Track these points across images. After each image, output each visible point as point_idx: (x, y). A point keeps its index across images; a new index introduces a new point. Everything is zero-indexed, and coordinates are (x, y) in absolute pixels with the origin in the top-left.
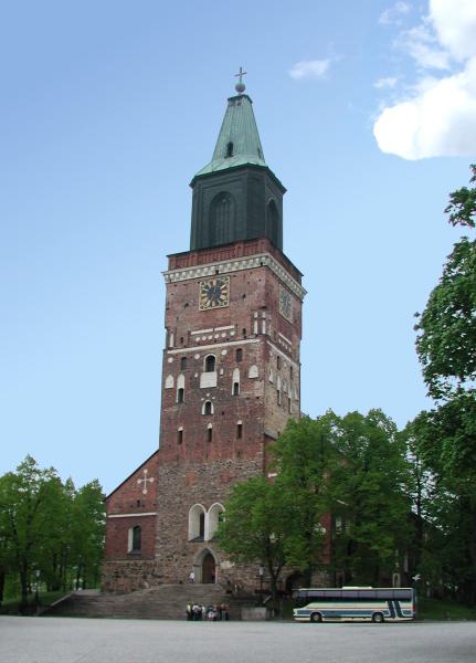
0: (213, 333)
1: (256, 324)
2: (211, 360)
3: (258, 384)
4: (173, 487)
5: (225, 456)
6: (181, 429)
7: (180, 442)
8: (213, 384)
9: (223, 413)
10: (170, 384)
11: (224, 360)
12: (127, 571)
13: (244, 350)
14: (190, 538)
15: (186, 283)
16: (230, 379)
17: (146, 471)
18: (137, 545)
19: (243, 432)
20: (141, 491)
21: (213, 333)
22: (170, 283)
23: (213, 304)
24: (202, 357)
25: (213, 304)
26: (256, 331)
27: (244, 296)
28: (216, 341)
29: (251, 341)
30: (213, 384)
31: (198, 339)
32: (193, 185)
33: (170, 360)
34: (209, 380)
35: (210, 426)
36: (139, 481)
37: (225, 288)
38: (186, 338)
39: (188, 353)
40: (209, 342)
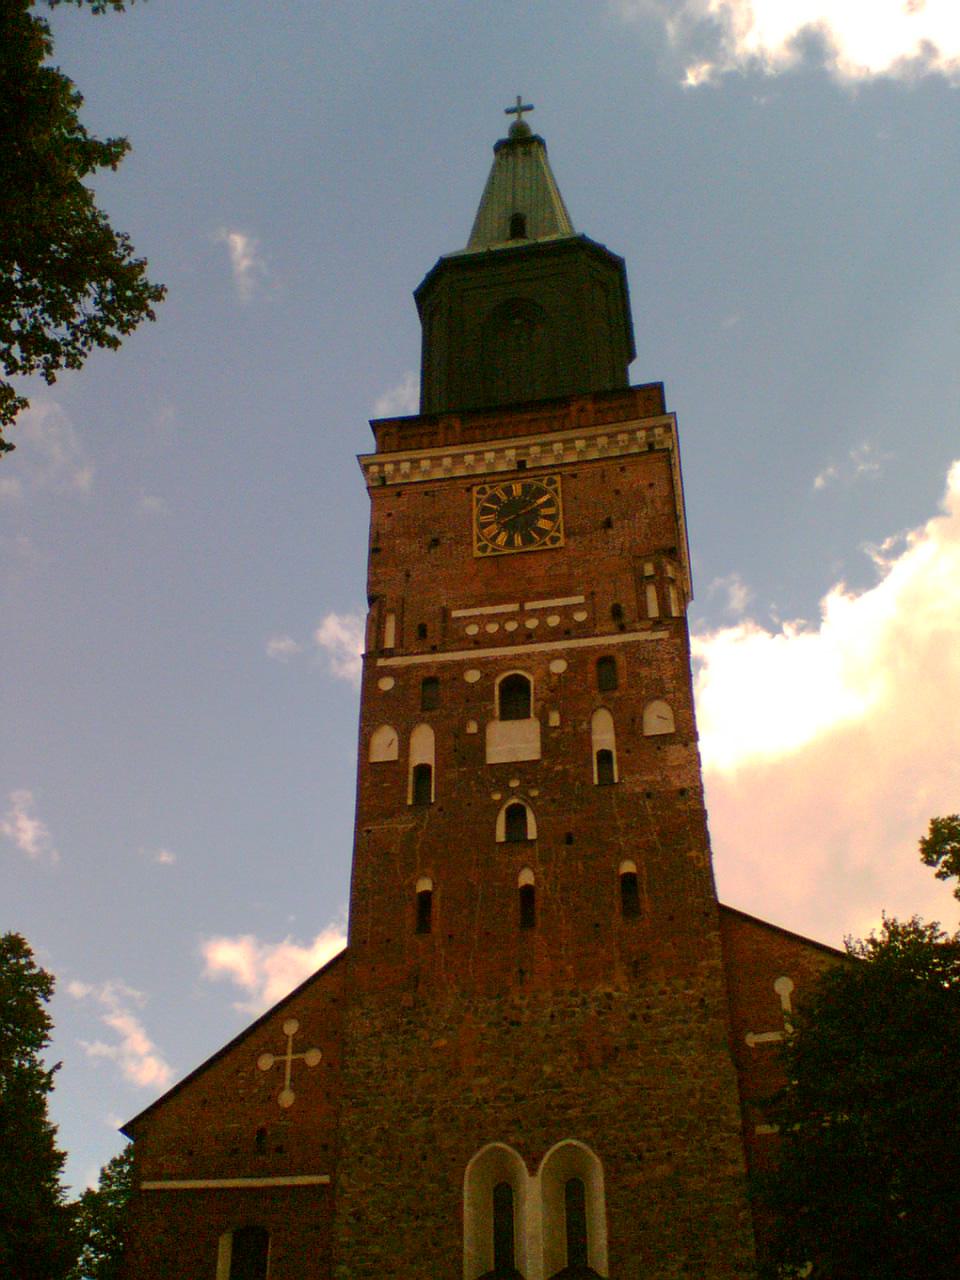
0: (522, 614)
1: (651, 593)
3: (675, 754)
6: (425, 885)
10: (385, 745)
11: (561, 693)
15: (430, 489)
16: (585, 739)
17: (291, 1028)
20: (272, 1099)
21: (522, 614)
22: (380, 488)
23: (518, 540)
24: (486, 676)
25: (518, 540)
26: (653, 611)
27: (608, 524)
28: (529, 637)
29: (642, 636)
31: (472, 630)
32: (425, 296)
33: (387, 684)
34: (513, 742)
35: (526, 878)
36: (266, 1062)
37: (549, 503)
38: (434, 629)
39: (443, 666)
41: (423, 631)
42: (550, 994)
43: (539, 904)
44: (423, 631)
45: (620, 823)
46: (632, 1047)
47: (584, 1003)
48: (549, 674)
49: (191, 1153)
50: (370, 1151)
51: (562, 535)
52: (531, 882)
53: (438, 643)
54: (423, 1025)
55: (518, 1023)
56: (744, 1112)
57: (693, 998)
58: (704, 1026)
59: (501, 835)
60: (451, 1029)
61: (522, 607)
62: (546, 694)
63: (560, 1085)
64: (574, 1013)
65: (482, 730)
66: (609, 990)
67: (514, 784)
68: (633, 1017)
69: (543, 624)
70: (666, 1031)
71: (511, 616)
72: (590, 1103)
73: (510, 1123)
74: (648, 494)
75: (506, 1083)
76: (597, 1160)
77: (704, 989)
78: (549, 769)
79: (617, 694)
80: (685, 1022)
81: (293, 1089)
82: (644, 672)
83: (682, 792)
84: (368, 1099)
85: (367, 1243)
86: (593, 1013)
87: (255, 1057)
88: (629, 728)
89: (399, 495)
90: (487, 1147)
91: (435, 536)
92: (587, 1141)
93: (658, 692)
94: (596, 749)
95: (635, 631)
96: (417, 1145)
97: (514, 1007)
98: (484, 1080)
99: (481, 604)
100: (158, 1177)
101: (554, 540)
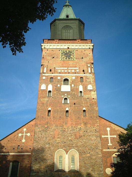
1: (89, 69)
2: (66, 80)
6: (50, 109)
8: (69, 90)
11: (73, 82)
13: (84, 78)
16: (78, 89)
17: (25, 130)
23: (68, 58)
25: (68, 58)
26: (90, 71)
27: (82, 58)
29: (88, 75)
30: (69, 90)
31: (59, 71)
34: (66, 88)
35: (67, 109)
39: (54, 76)
40: (66, 73)
41: (51, 70)
42: (71, 127)
44: (51, 70)
45: (83, 102)
47: (76, 128)
48: (72, 79)
51: (75, 59)
53: (53, 73)
54: (48, 130)
56: (102, 147)
57: (94, 129)
59: (63, 102)
60: (53, 131)
61: (68, 68)
62: (71, 82)
63: (72, 141)
65: (60, 86)
67: (66, 95)
68: (85, 131)
69: (71, 71)
70: (90, 134)
71: (66, 70)
72: (77, 144)
74: (89, 55)
75: (63, 140)
76: (78, 153)
78: (72, 93)
79: (83, 83)
82: (88, 80)
83: (93, 98)
84: (38, 141)
86: (78, 130)
87: (18, 134)
88: (85, 88)
89: (47, 50)
90: (59, 150)
91: (54, 57)
92: (76, 149)
93: (91, 84)
94: (80, 91)
95: (86, 74)
98: (59, 139)
99: (61, 67)
101: (74, 59)
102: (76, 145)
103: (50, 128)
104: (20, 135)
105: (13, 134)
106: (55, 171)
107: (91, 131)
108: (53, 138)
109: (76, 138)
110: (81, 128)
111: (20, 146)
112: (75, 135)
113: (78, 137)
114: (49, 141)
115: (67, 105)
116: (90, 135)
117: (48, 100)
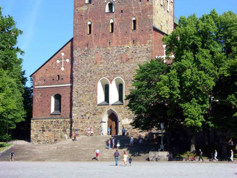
4: (85, 65)
5: (124, 43)
6: (89, 23)
7: (90, 32)
9: (122, 11)
12: (51, 127)
14: (99, 102)
18: (58, 107)
19: (137, 26)
42: (115, 47)
43: (114, 27)
45: (134, 8)
46: (132, 58)
49: (45, 80)
50: (79, 79)
52: (113, 22)
54: (89, 54)
55: (109, 53)
58: (147, 54)
63: (117, 66)
64: (120, 51)
66: (128, 46)
68: (133, 52)
70: (139, 55)
73: (107, 74)
75: (106, 66)
76: (123, 81)
77: (148, 47)
80: (143, 53)
81: (64, 67)
85: (79, 97)
86: (124, 51)
87: (56, 60)
90: (102, 78)
92: (122, 77)
96: (89, 78)
97: (108, 50)
98: (102, 65)
100: (38, 85)
102: (121, 71)
103: (91, 51)
104: (58, 61)
105: (50, 61)
106: (98, 103)
107: (140, 51)
108: (95, 64)
109: (122, 62)
110: (128, 48)
111: (60, 76)
112: (121, 58)
113: (125, 61)
114: (90, 67)
115: (112, 15)
116: (139, 57)
117: (86, 9)
